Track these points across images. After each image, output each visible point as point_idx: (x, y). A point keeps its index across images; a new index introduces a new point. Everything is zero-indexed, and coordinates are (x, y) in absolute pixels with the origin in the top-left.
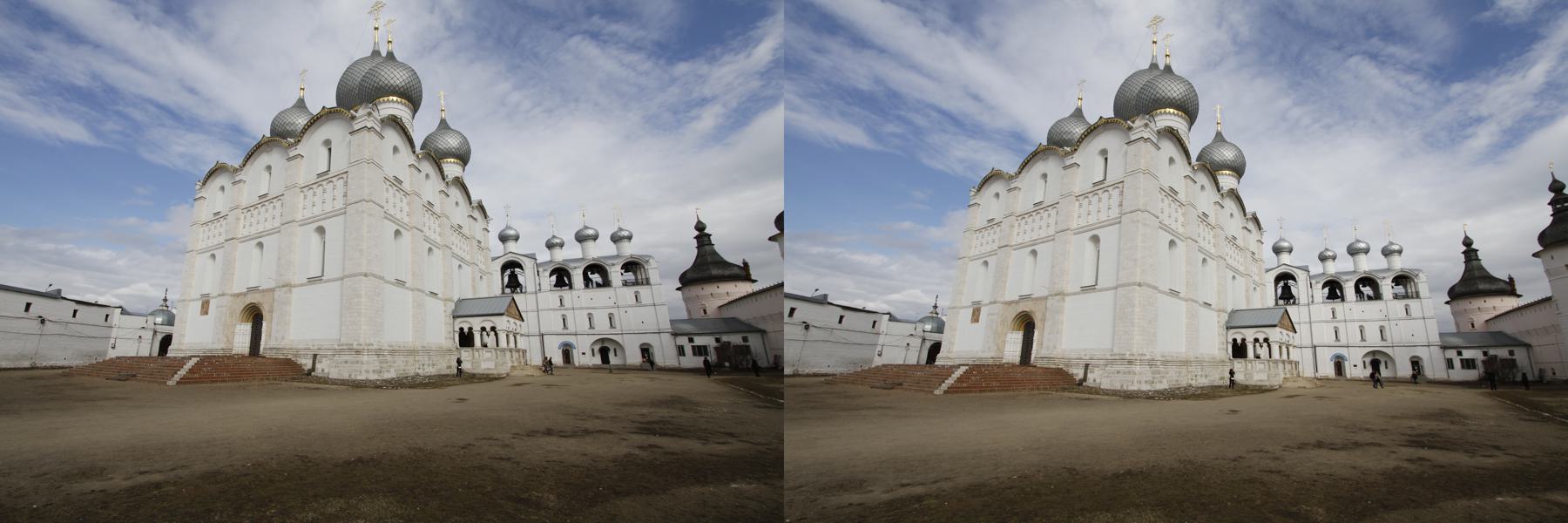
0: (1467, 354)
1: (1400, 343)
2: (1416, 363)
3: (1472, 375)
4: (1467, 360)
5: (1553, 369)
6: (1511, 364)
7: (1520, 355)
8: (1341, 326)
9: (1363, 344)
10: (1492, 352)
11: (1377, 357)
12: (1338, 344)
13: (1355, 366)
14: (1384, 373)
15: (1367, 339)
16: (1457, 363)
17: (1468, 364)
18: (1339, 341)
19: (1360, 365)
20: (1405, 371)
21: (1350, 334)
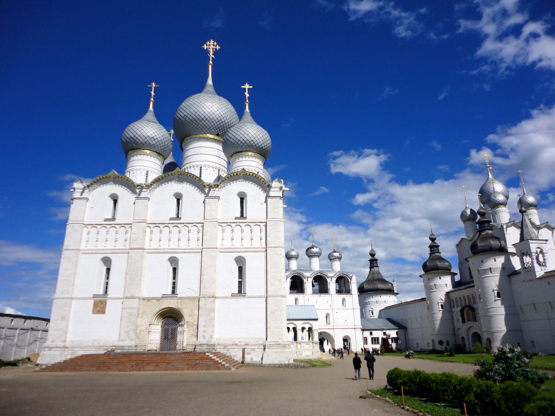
4: (375, 338)
5: (417, 343)
10: (388, 332)
16: (369, 341)
17: (375, 340)
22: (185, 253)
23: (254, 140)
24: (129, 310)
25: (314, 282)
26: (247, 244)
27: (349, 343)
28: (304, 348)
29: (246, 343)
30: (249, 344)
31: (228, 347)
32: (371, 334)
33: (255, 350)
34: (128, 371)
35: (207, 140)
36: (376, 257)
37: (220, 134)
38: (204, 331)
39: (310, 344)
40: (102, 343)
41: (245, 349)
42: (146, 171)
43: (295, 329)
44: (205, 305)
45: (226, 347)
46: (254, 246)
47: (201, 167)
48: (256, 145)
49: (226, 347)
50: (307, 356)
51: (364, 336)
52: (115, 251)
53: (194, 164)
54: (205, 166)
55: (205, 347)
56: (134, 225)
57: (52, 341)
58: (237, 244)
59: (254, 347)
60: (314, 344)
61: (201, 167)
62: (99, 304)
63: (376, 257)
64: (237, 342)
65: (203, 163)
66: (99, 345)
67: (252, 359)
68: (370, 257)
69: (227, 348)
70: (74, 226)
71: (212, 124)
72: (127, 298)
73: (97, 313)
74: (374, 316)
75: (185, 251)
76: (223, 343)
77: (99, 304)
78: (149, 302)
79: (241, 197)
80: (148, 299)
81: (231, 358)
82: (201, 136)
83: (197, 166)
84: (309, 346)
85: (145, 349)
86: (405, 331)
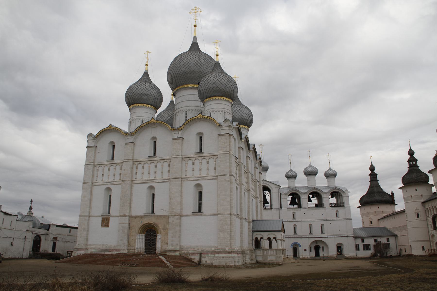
0: (367, 241)
1: (332, 235)
2: (339, 248)
3: (367, 253)
4: (366, 245)
6: (387, 246)
7: (392, 241)
8: (298, 225)
9: (311, 236)
10: (379, 240)
11: (318, 244)
12: (296, 236)
13: (305, 250)
14: (322, 254)
15: (313, 233)
16: (361, 247)
17: (367, 247)
18: (296, 234)
19: (308, 250)
20: (333, 252)
21: (303, 229)
22: (159, 182)
23: (219, 87)
24: (123, 225)
25: (312, 198)
26: (204, 174)
27: (343, 249)
28: (269, 254)
29: (203, 249)
30: (205, 250)
31: (190, 252)
32: (363, 241)
33: (209, 255)
34: (106, 265)
35: (191, 89)
36: (375, 171)
38: (173, 241)
39: (274, 252)
40: (108, 247)
41: (202, 254)
43: (269, 239)
44: (173, 221)
45: (189, 252)
46: (210, 175)
48: (221, 90)
49: (189, 252)
50: (272, 260)
51: (356, 243)
52: (114, 183)
53: (182, 109)
54: (189, 110)
55: (172, 252)
56: (124, 164)
57: (78, 245)
58: (197, 174)
59: (208, 252)
60: (277, 251)
61: (186, 112)
62: (105, 220)
63: (375, 171)
64: (196, 249)
65: (188, 108)
66: (106, 248)
67: (206, 262)
68: (370, 172)
69: (189, 253)
70: (88, 167)
71: (193, 76)
72: (121, 216)
73: (104, 227)
74: (373, 225)
75: (159, 181)
76: (186, 249)
77: (105, 220)
78: (136, 219)
80: (136, 217)
81: (192, 260)
82: (185, 86)
84: (261, 252)
85: (134, 252)
86: (396, 238)
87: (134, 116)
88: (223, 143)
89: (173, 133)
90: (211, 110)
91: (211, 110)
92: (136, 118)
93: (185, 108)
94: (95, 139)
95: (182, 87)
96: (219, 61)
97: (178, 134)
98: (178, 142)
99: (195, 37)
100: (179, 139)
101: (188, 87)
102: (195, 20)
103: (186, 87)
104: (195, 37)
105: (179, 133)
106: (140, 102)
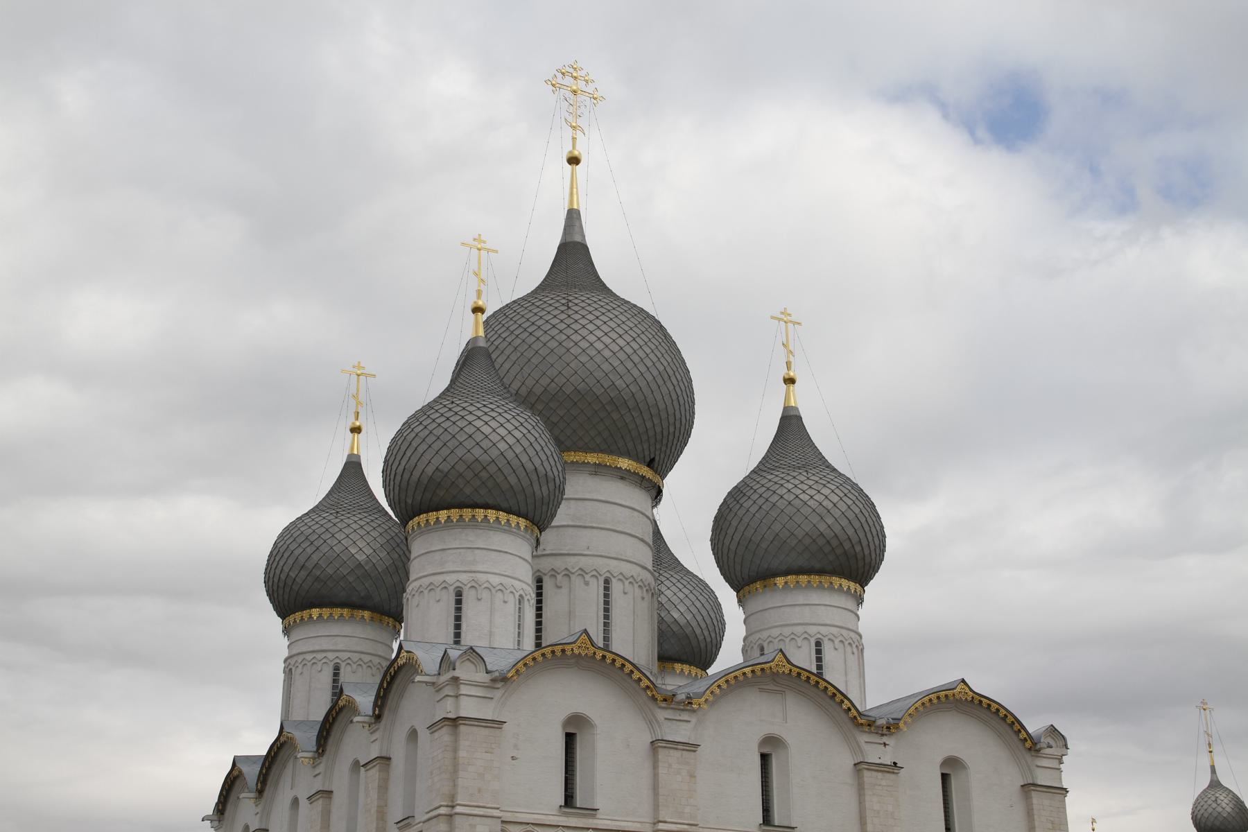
35: (622, 478)
37: (657, 459)
42: (517, 596)
47: (607, 581)
53: (583, 562)
54: (623, 578)
61: (607, 581)
79: (943, 772)
82: (608, 459)
83: (595, 573)
87: (480, 568)
88: (1050, 826)
89: (863, 738)
90: (824, 630)
91: (824, 630)
92: (495, 580)
93: (604, 566)
94: (499, 685)
95: (592, 458)
96: (797, 409)
97: (882, 746)
98: (883, 783)
99: (573, 217)
100: (888, 772)
101: (616, 467)
102: (574, 128)
103: (610, 466)
104: (573, 217)
105: (885, 744)
106: (479, 500)
